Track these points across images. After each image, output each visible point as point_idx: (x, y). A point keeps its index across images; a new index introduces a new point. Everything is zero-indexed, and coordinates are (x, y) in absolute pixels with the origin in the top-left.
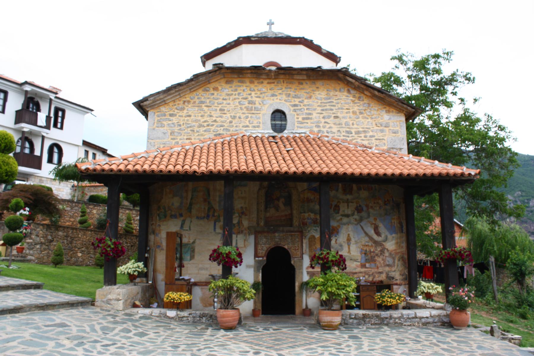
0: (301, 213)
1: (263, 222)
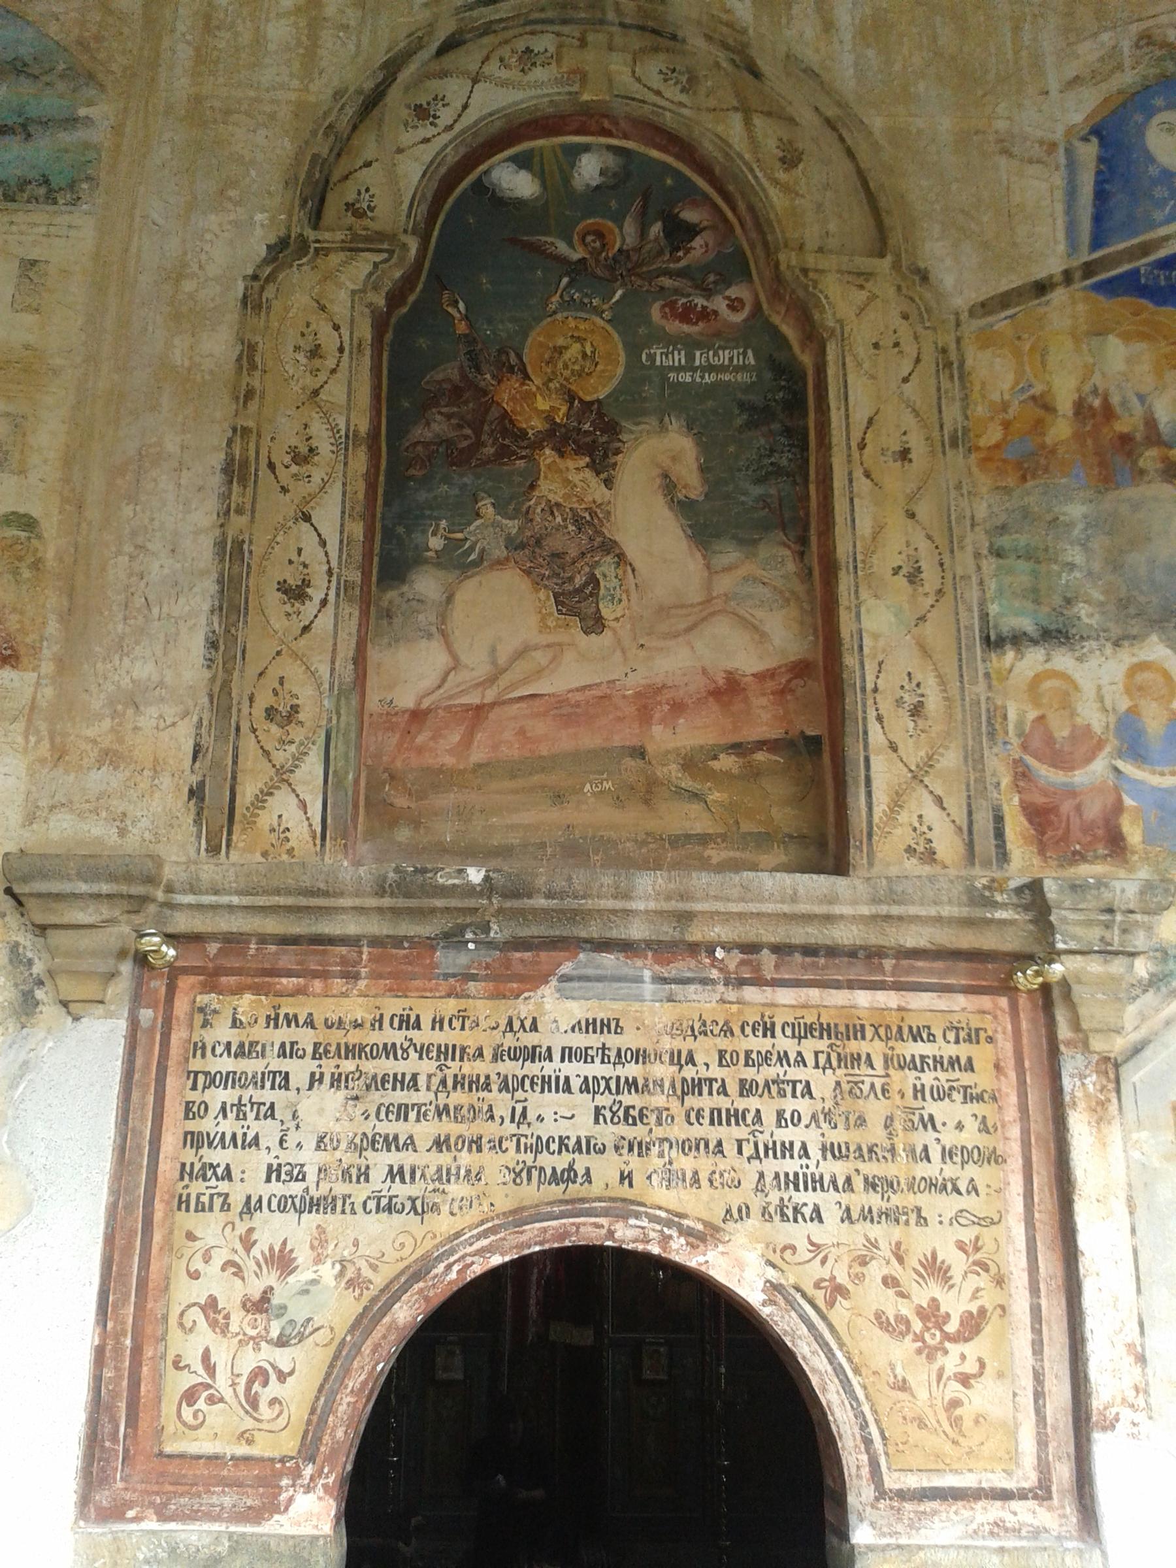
0: (993, 642)
1: (312, 768)
